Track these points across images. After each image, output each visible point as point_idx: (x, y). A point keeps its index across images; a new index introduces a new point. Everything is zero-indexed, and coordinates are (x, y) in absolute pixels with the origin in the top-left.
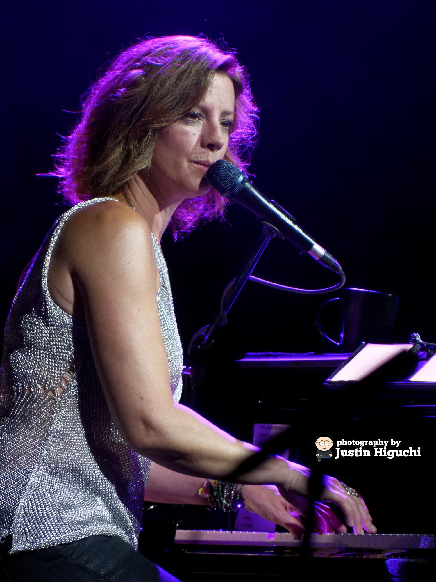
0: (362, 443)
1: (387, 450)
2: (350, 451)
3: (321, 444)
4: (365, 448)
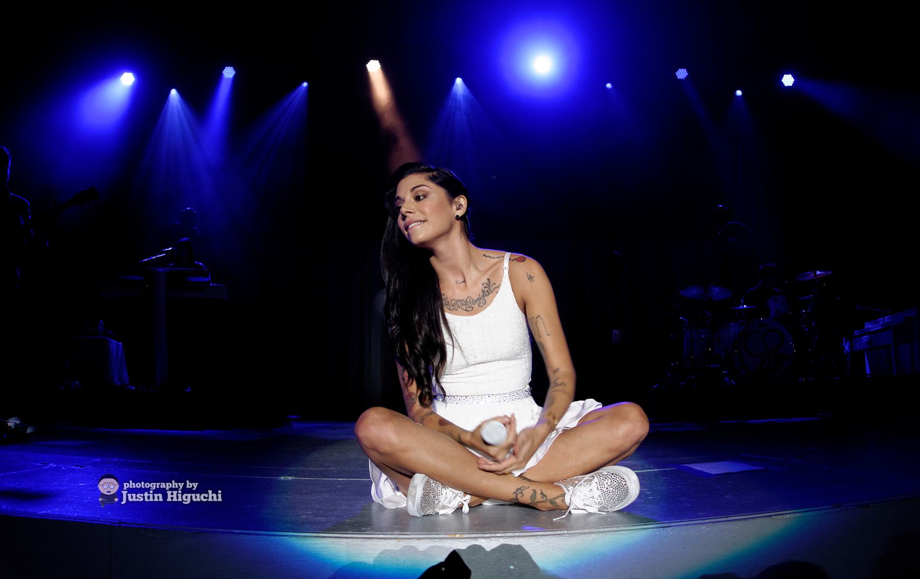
0: (153, 486)
1: (182, 494)
4: (157, 491)
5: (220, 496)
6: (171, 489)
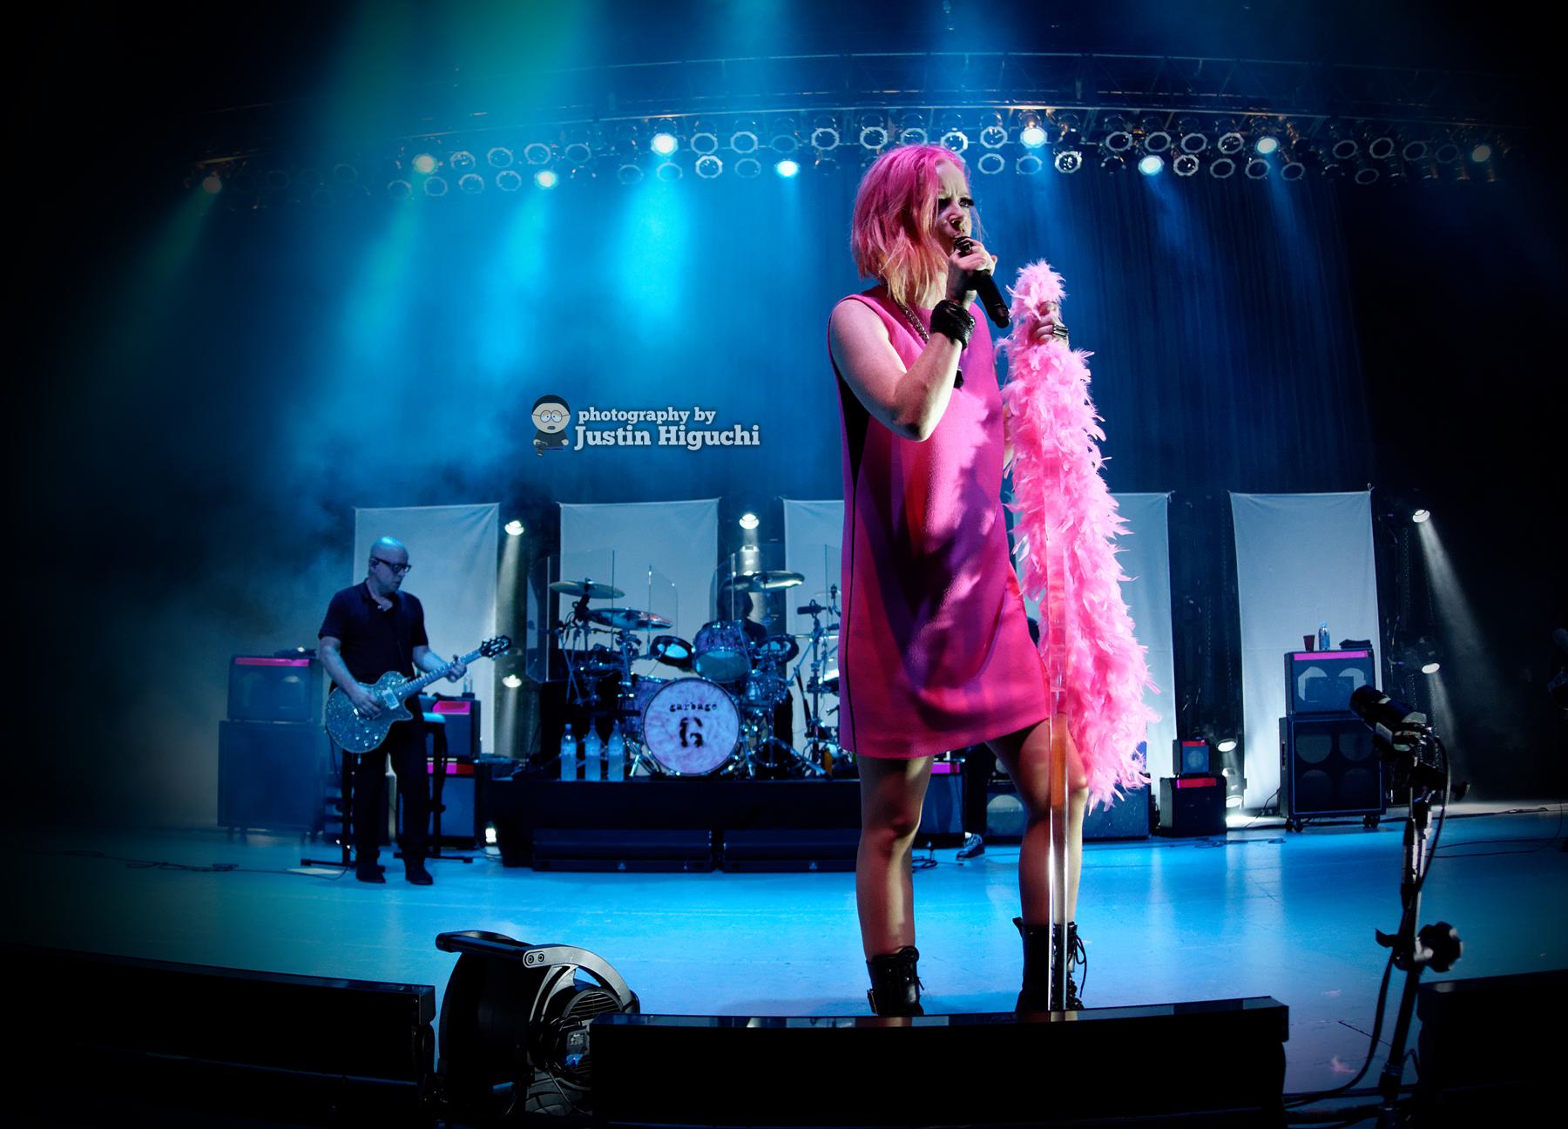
0: (633, 417)
2: (605, 435)
3: (545, 419)
5: (755, 435)
6: (665, 423)
